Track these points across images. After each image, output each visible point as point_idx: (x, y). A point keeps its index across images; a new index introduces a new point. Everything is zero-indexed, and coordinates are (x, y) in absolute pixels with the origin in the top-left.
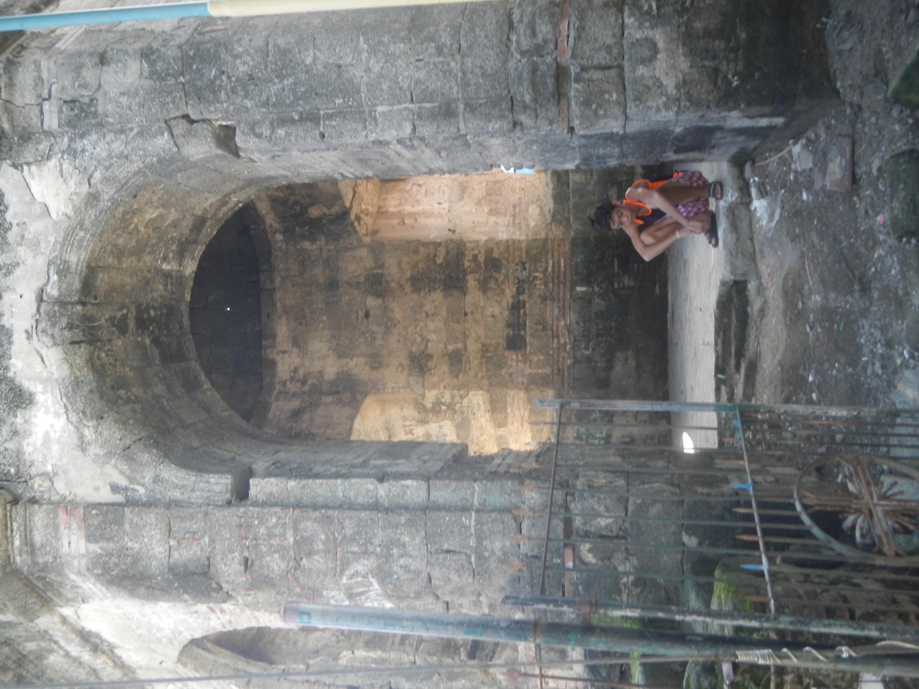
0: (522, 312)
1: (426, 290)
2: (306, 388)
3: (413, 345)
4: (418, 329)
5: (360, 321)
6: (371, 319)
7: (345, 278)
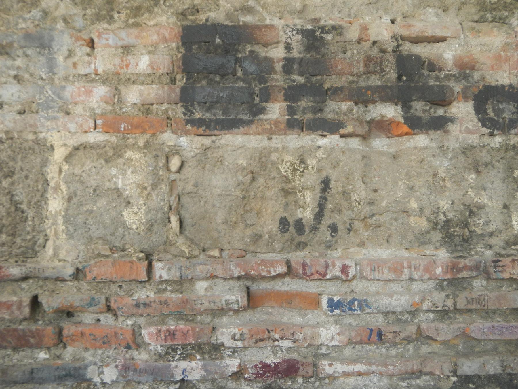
0: (391, 111)
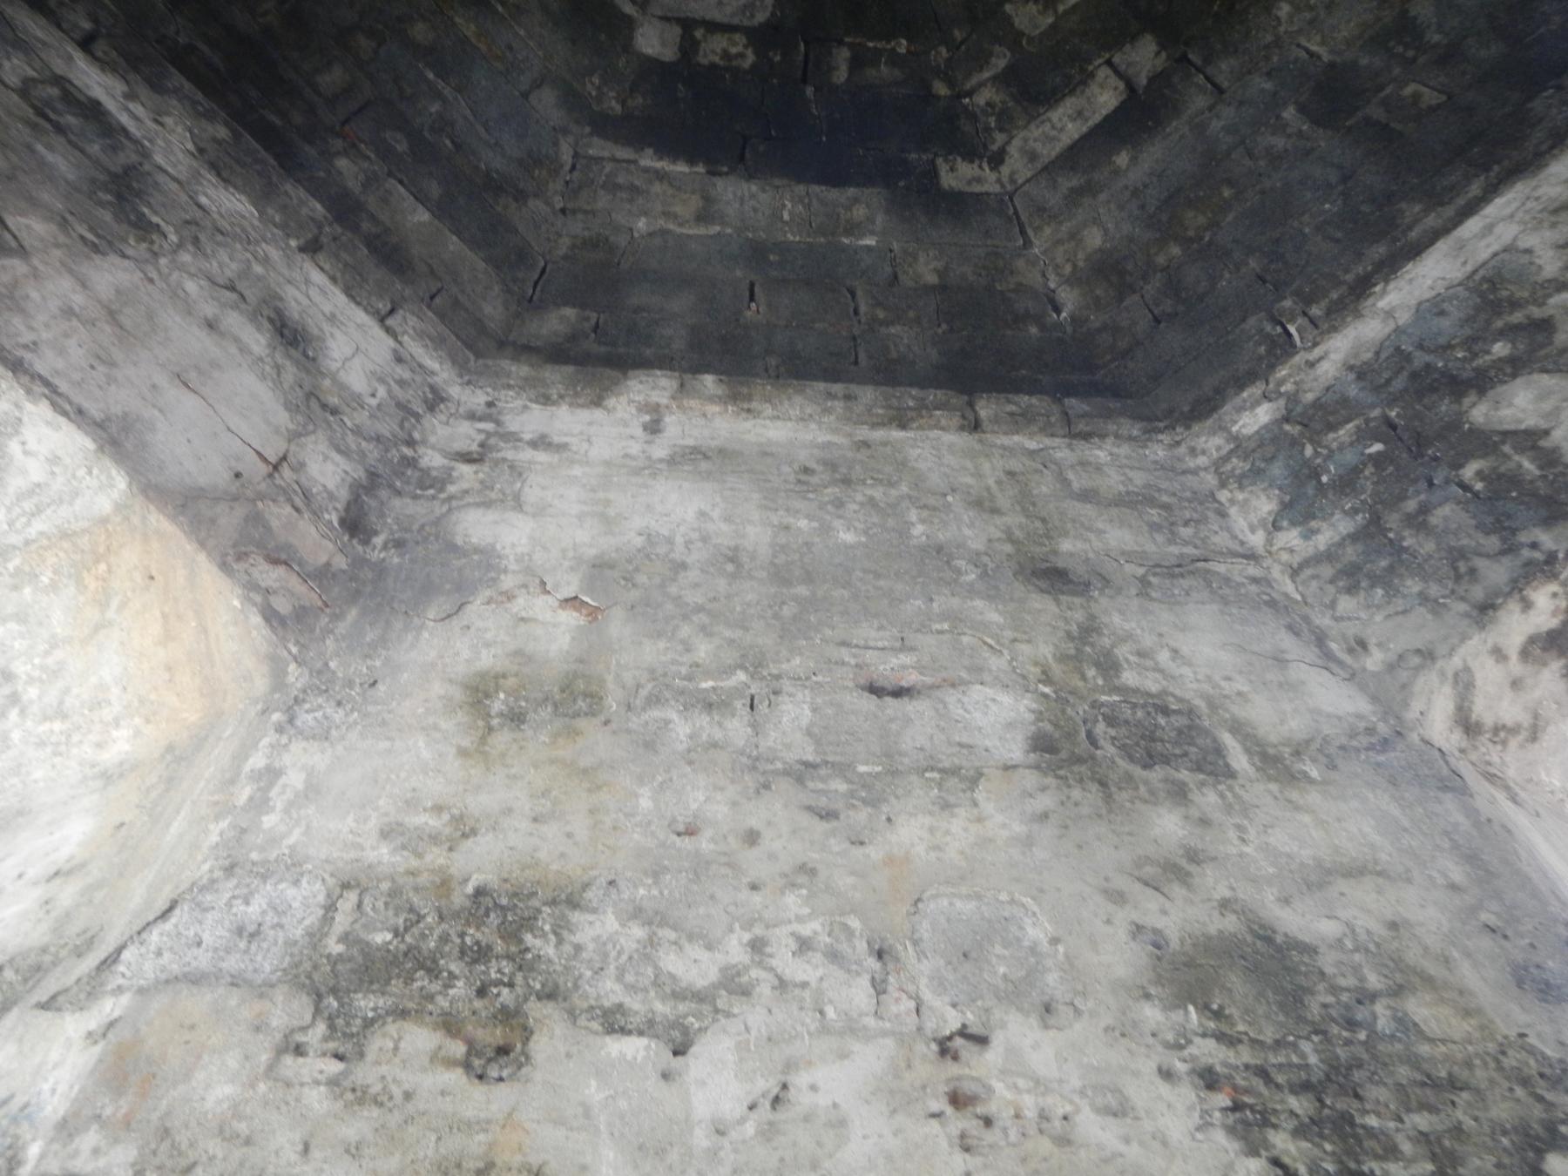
1: (1208, 1051)
3: (636, 913)
4: (785, 961)
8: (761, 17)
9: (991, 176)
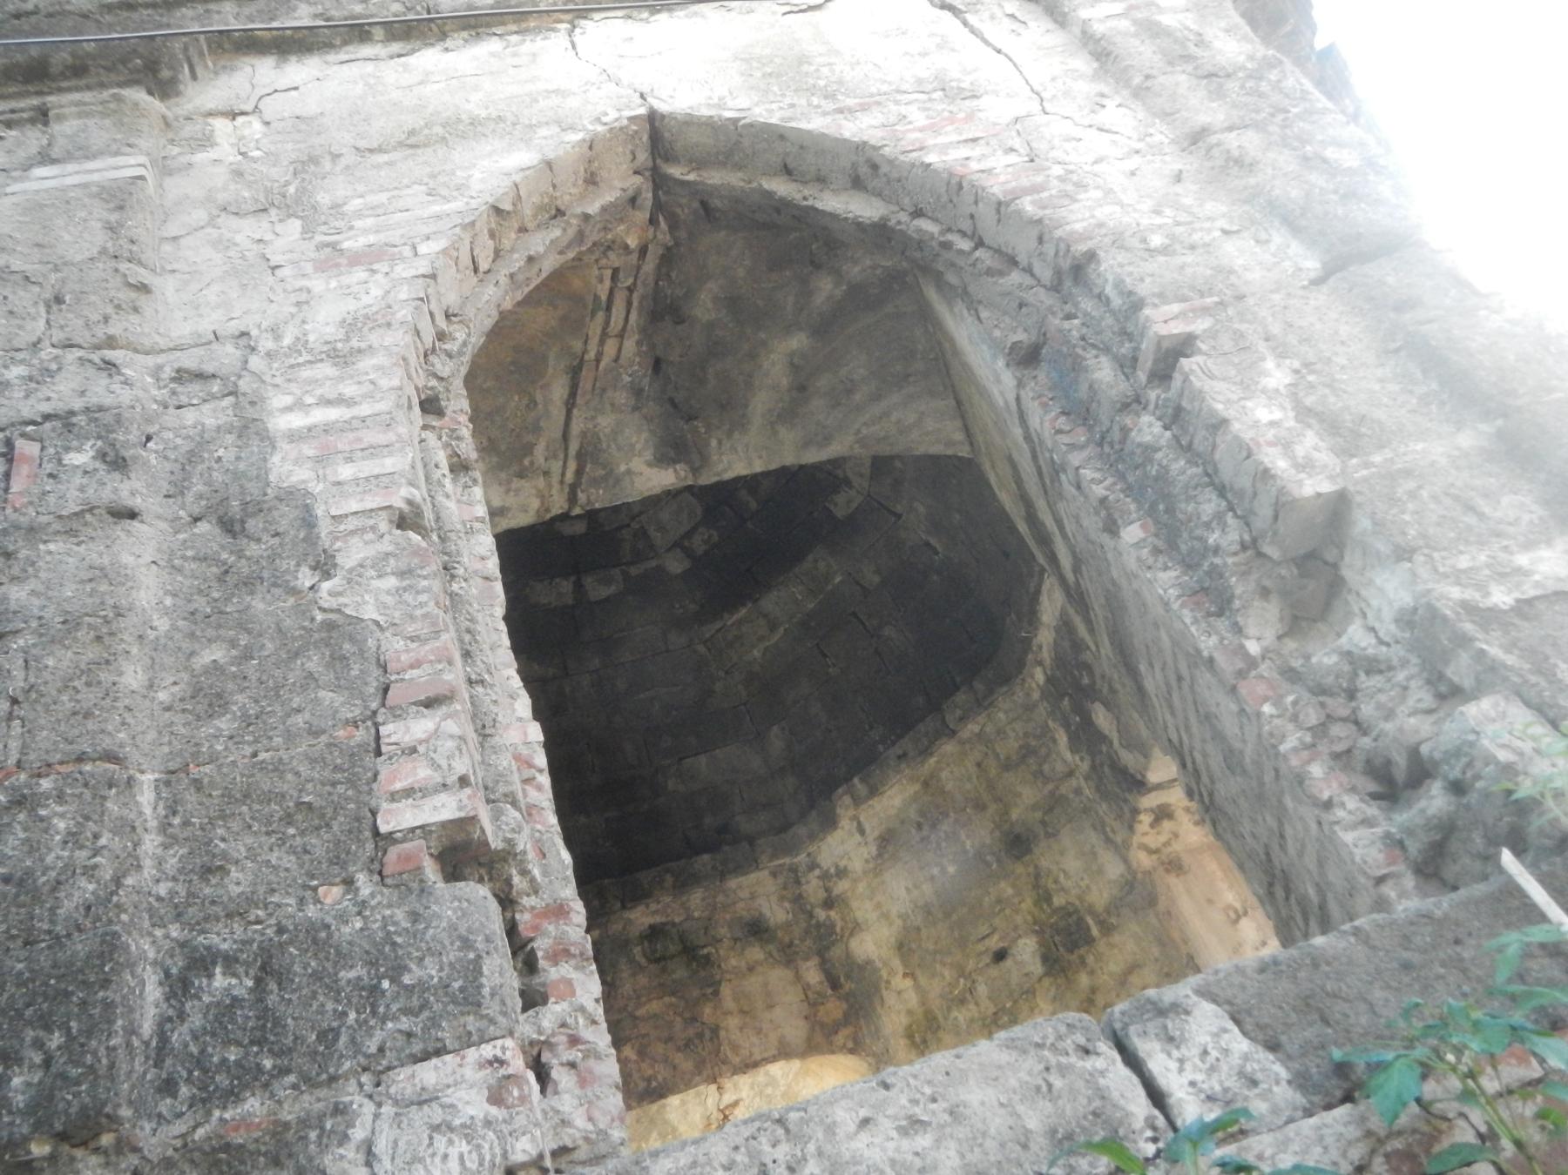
2: (821, 914)
5: (981, 947)
6: (994, 972)
7: (1044, 863)
8: (699, 511)
9: (853, 493)
